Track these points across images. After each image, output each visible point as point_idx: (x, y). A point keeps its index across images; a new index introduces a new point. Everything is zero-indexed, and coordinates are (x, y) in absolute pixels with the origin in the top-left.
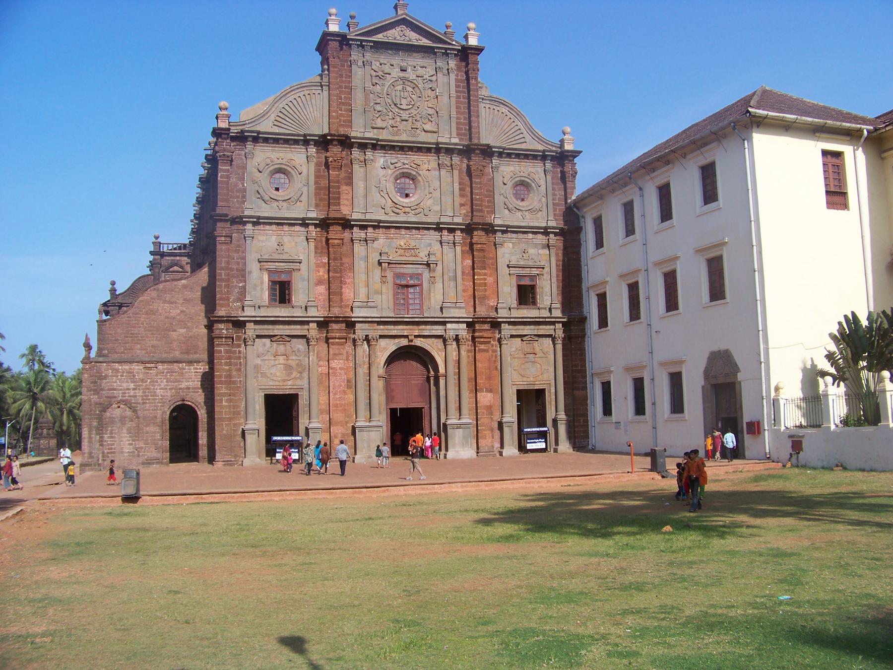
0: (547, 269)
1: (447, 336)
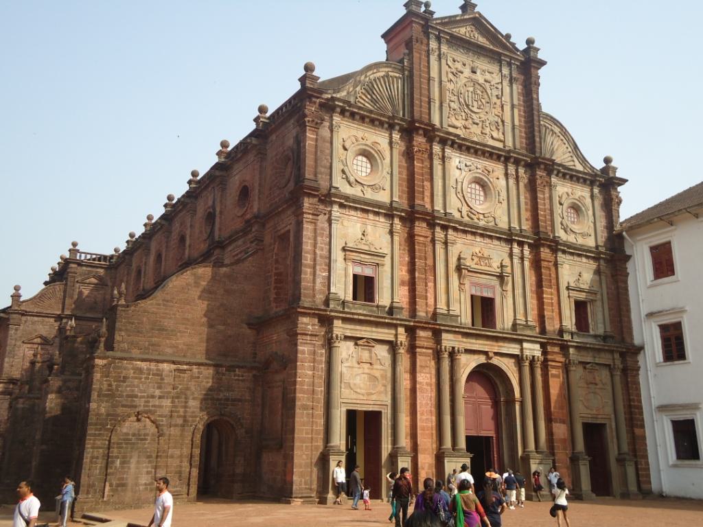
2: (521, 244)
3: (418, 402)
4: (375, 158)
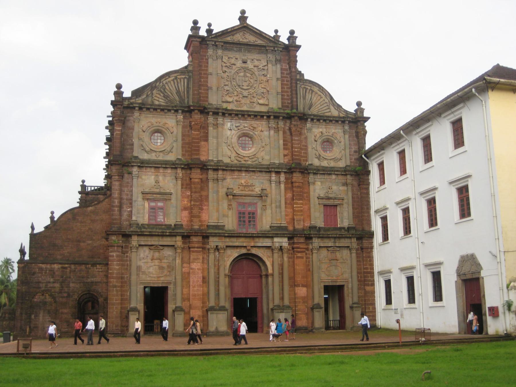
0: (345, 201)
1: (274, 247)
2: (278, 173)
3: (191, 280)
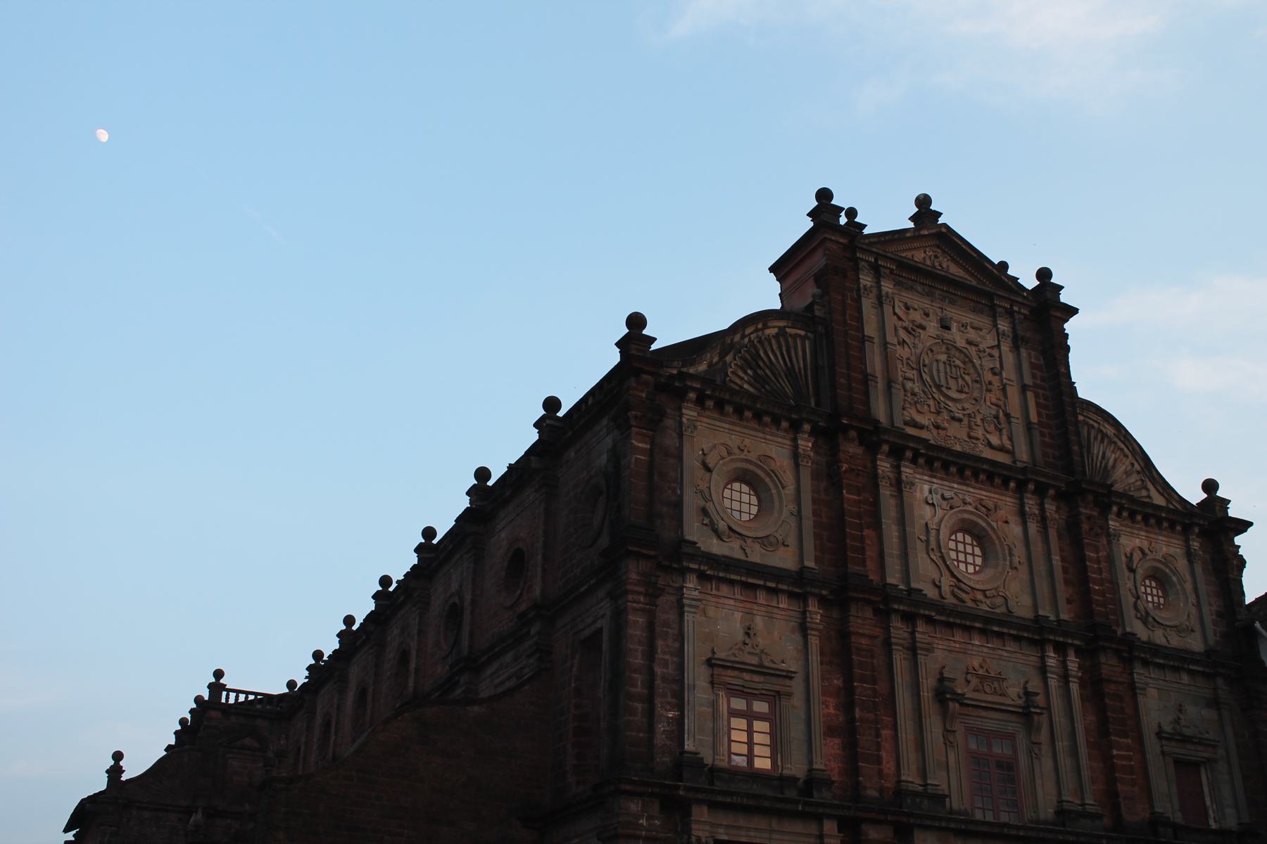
2: (1061, 649)
4: (766, 484)
